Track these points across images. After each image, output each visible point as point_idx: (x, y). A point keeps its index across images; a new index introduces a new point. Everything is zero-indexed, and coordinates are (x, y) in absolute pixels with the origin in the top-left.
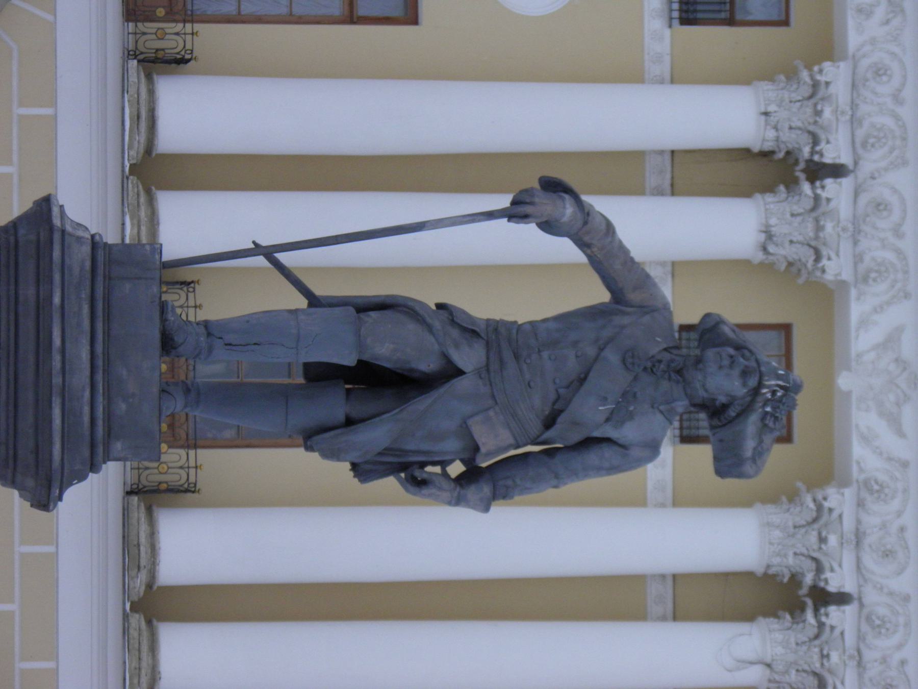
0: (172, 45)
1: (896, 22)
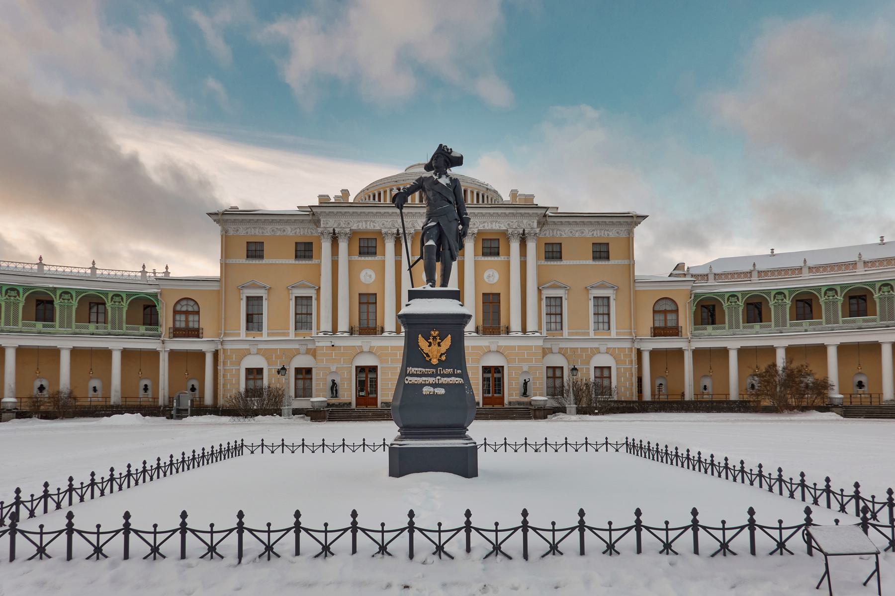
0: (380, 329)
1: (376, 222)
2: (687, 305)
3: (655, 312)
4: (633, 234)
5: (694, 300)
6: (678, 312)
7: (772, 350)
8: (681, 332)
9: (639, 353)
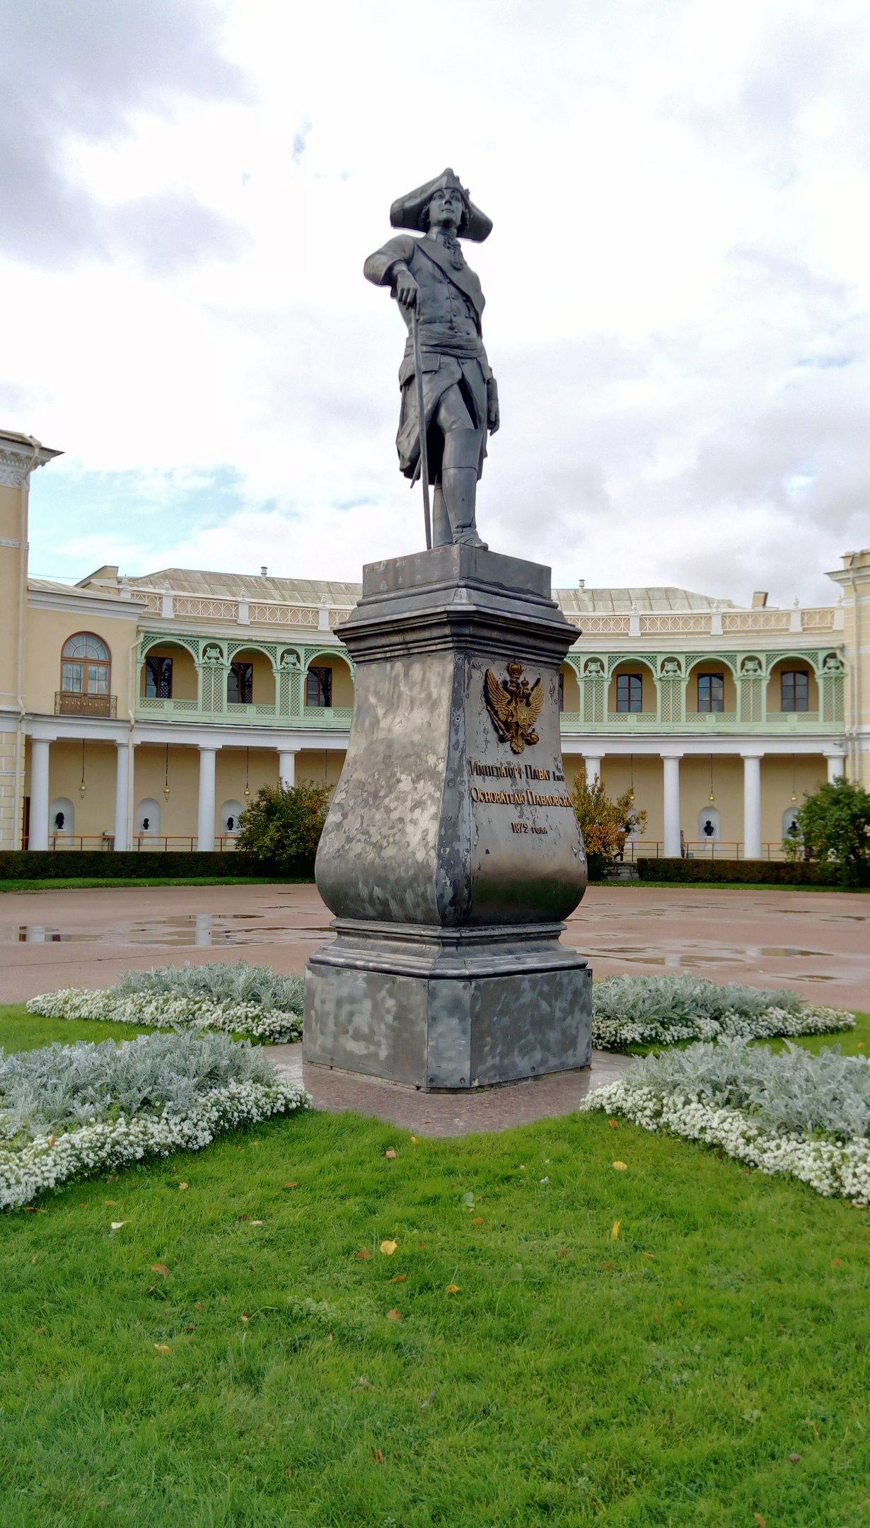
2: (131, 653)
3: (64, 660)
4: (28, 484)
5: (143, 645)
6: (110, 665)
7: (271, 756)
8: (116, 707)
9: (29, 743)
